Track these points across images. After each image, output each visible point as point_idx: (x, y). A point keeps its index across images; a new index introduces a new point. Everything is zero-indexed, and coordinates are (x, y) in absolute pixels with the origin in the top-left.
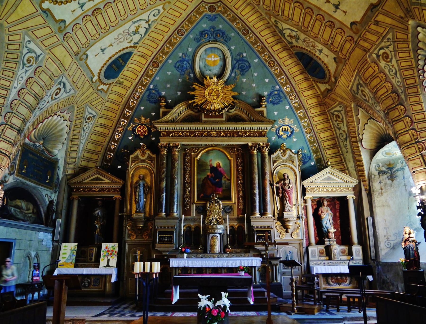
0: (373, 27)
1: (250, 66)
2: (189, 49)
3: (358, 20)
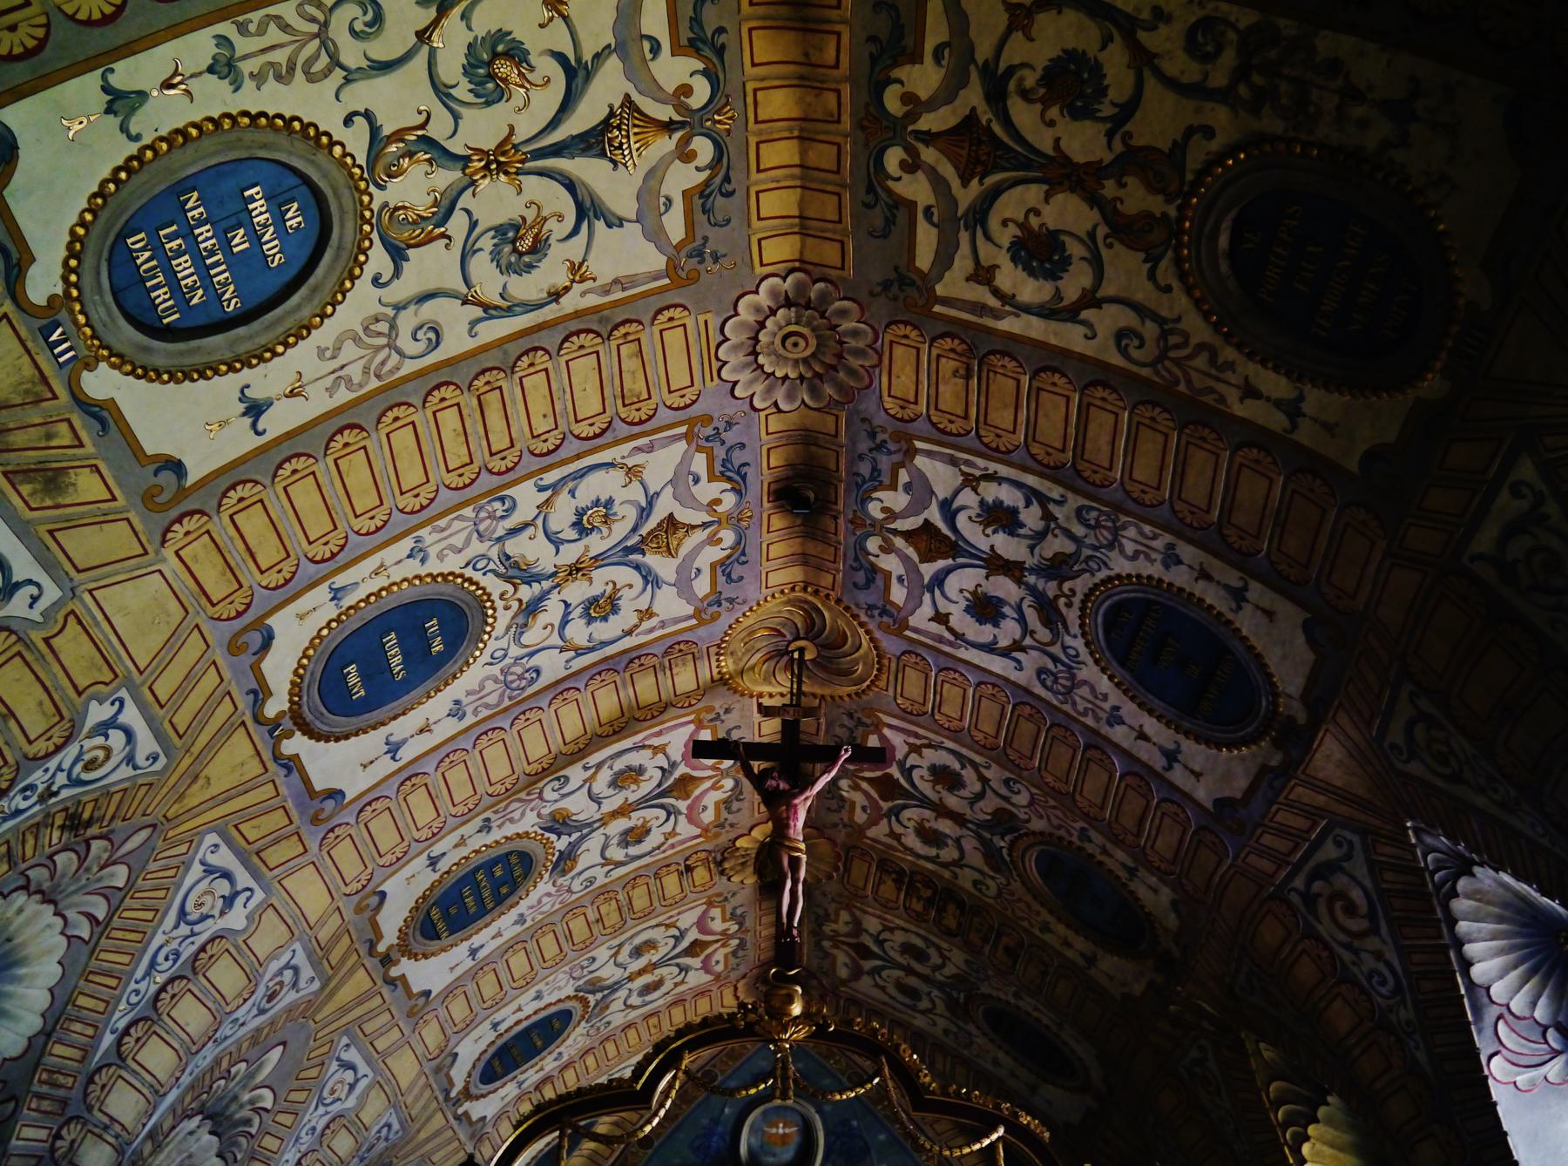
2: (727, 1110)
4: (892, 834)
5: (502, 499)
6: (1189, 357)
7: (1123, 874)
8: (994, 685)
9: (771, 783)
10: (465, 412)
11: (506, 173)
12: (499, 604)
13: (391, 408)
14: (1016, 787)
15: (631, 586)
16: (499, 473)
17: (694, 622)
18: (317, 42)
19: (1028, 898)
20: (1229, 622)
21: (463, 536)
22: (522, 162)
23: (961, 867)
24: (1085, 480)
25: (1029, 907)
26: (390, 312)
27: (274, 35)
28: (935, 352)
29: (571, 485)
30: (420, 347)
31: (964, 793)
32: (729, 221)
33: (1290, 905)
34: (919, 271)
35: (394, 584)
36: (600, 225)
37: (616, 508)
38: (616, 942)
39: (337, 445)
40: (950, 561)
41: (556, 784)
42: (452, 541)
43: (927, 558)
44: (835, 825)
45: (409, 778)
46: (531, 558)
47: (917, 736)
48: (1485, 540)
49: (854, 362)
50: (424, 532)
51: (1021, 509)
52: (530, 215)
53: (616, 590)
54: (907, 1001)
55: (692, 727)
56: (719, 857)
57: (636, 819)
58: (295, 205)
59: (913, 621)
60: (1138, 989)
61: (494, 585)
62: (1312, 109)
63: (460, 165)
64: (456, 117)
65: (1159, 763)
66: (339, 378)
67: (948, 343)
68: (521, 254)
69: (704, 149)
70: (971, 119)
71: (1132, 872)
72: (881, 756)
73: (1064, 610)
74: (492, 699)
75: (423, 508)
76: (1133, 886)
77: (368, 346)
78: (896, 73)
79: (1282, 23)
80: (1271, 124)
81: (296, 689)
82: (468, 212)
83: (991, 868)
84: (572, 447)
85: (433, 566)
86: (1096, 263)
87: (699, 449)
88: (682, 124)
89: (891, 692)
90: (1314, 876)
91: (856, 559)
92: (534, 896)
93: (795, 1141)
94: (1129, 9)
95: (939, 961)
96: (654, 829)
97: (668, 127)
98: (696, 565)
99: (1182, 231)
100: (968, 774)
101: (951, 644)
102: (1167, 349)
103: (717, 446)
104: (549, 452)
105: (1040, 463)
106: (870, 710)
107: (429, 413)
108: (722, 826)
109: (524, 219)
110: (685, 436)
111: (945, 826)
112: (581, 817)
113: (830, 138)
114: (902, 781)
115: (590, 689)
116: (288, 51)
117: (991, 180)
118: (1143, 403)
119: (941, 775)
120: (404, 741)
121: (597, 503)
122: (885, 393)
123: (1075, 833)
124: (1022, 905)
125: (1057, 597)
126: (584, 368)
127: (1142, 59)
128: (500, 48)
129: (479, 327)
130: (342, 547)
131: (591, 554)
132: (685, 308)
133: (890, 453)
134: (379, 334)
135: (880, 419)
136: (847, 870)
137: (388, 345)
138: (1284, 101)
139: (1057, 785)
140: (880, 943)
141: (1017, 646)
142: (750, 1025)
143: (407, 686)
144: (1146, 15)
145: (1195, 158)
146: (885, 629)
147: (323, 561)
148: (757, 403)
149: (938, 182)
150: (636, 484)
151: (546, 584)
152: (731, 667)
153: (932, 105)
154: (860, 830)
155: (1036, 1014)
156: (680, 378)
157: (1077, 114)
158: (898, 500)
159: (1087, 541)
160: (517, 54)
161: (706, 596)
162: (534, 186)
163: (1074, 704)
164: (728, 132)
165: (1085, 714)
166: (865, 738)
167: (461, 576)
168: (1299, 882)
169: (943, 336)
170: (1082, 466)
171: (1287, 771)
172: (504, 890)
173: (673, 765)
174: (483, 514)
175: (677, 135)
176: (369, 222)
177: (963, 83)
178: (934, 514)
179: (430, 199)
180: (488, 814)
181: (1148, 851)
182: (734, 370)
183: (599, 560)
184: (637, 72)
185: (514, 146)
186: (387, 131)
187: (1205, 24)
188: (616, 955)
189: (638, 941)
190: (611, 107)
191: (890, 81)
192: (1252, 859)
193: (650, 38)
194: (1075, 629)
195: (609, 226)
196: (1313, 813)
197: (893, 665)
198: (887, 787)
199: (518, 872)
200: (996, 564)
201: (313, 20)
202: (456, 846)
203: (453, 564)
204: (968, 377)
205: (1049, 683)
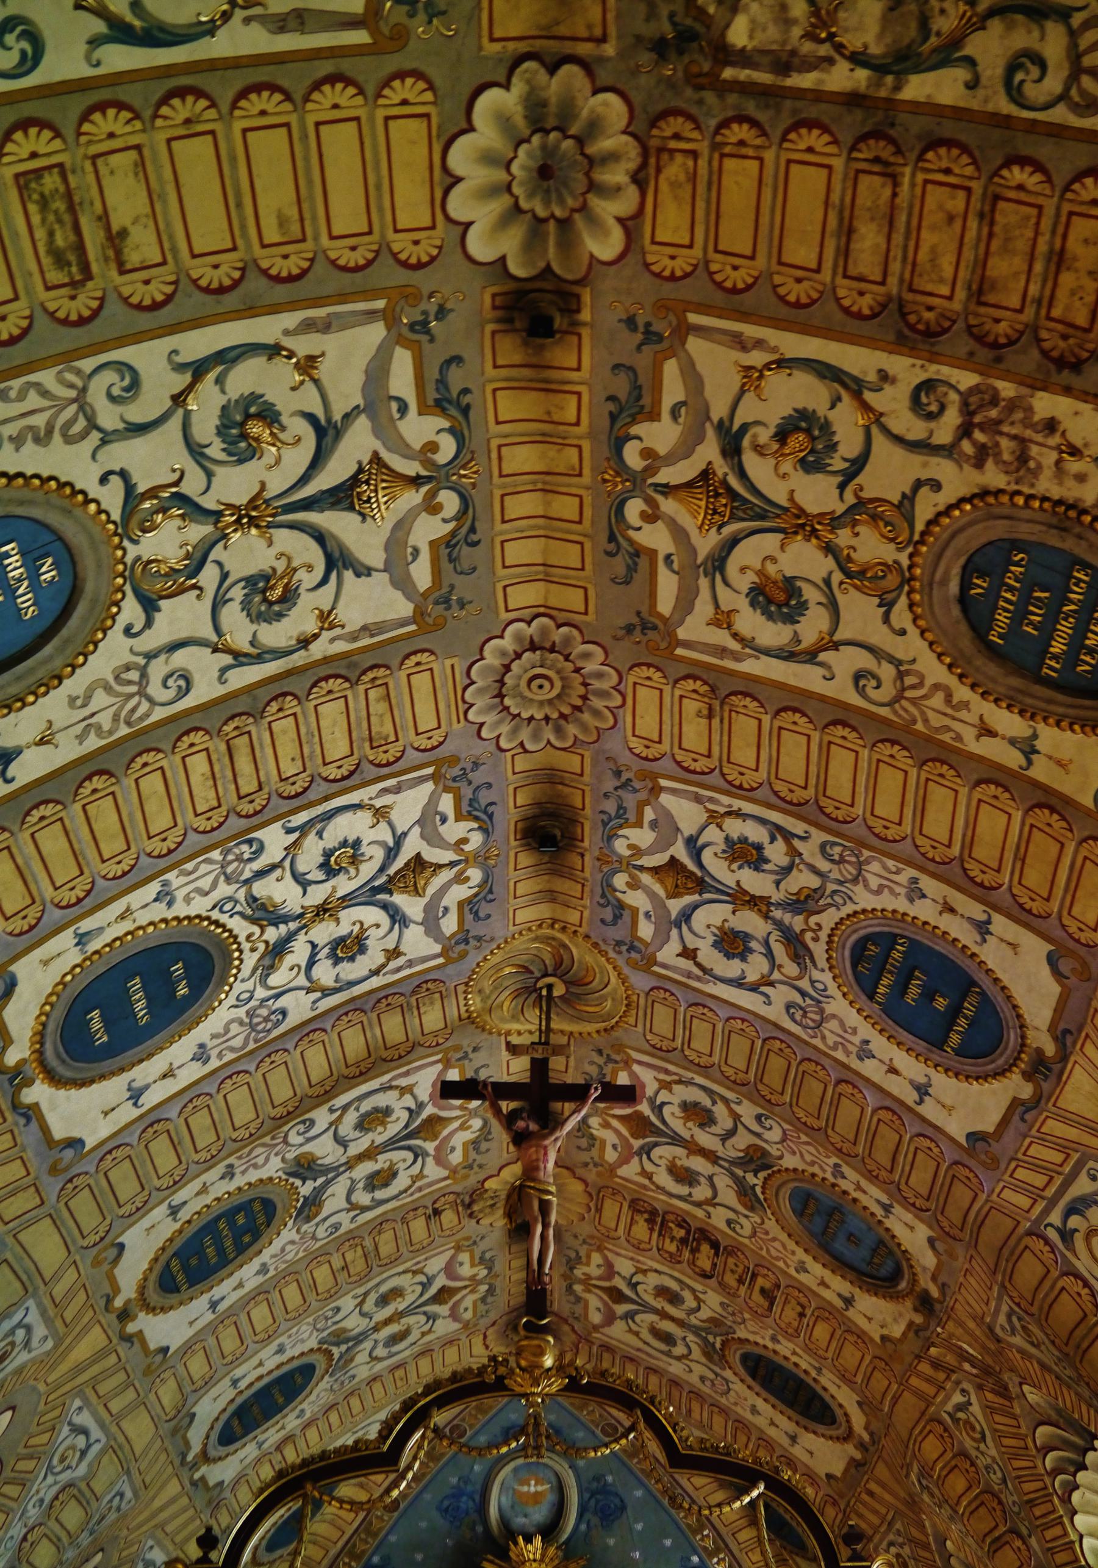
0: (864, 1496)
1: (623, 1508)
2: (476, 1468)
3: (839, 1474)
4: (644, 1173)
5: (250, 842)
6: (925, 697)
7: (879, 1212)
8: (743, 1020)
9: (521, 1124)
10: (214, 757)
11: (257, 527)
12: (246, 946)
13: (140, 754)
14: (768, 1123)
15: (378, 926)
16: (247, 816)
17: (441, 960)
18: (74, 407)
19: (783, 1237)
20: (974, 955)
21: (210, 879)
22: (273, 515)
23: (715, 1205)
24: (828, 816)
25: (784, 1246)
26: (142, 661)
27: (33, 400)
28: (677, 693)
29: (319, 826)
30: (171, 694)
31: (714, 1129)
32: (474, 569)
33: (1047, 1242)
34: (660, 616)
35: (140, 928)
36: (348, 574)
37: (364, 849)
38: (361, 1290)
39: (86, 791)
40: (696, 897)
41: (301, 1128)
42: (200, 884)
43: (674, 895)
44: (586, 1165)
45: (151, 1125)
46: (278, 899)
47: (667, 1072)
49: (597, 703)
50: (170, 876)
51: (766, 845)
52: (280, 567)
53: (363, 930)
54: (663, 1347)
55: (440, 1066)
56: (467, 1200)
57: (382, 1162)
58: (50, 560)
59: (661, 956)
60: (897, 1331)
61: (240, 927)
62: (1032, 464)
63: (212, 519)
64: (209, 475)
65: (910, 1096)
66: (89, 727)
67: (690, 684)
68: (271, 604)
69: (450, 501)
70: (706, 474)
71: (887, 1209)
72: (629, 1094)
73: (811, 945)
74: (237, 1042)
75: (170, 852)
76: (888, 1223)
77: (118, 695)
78: (634, 430)
79: (1000, 384)
80: (994, 477)
81: (40, 1036)
82: (220, 564)
83: (745, 1206)
84: (321, 788)
85: (181, 909)
86: (833, 607)
87: (447, 789)
88: (429, 479)
89: (640, 1028)
90: (1070, 1211)
91: (603, 895)
92: (277, 1244)
93: (551, 1498)
94: (855, 372)
95: (694, 1304)
96: (401, 1173)
97: (416, 481)
98: (444, 903)
99: (913, 578)
100: (720, 1111)
101: (698, 979)
102: (904, 689)
103: (463, 785)
104: (297, 795)
105: (783, 799)
106: (619, 1047)
107: (177, 759)
108: (471, 1167)
109: (274, 570)
110: (433, 777)
111: (698, 1164)
112: (327, 1161)
113: (574, 491)
114: (653, 1119)
115: (338, 1029)
116: (47, 415)
117: (728, 530)
118: (882, 741)
119: (690, 1109)
120: (147, 1087)
121: (344, 844)
122: (629, 733)
123: (829, 1170)
124: (776, 1244)
125: (803, 931)
126: (331, 711)
128: (253, 410)
129: (229, 674)
130: (89, 892)
131: (340, 893)
132: (432, 653)
133: (635, 791)
134: (130, 682)
135: (625, 758)
136: (599, 1210)
137: (139, 693)
138: (1006, 457)
139: (810, 1121)
140: (634, 1286)
141: (767, 981)
142: (500, 1379)
143: (151, 1030)
144: (872, 377)
145: (924, 511)
146: (635, 966)
147: (68, 906)
148: (504, 744)
149: (679, 533)
150: (383, 825)
151: (293, 926)
152: (479, 1005)
153: (671, 459)
154: (612, 1169)
155: (794, 1359)
156: (427, 721)
158: (643, 837)
159: (832, 876)
160: (269, 416)
161: (453, 935)
162: (285, 538)
163: (824, 1038)
164: (474, 485)
165: (835, 1048)
166: (615, 1073)
167: (208, 918)
168: (1055, 1218)
169: (686, 677)
170: (823, 802)
171: (1037, 1102)
172: (247, 1239)
173: (421, 1106)
174: (230, 857)
175: (424, 489)
176: (122, 575)
177: (700, 439)
178: (679, 851)
179: (183, 552)
180: (232, 1160)
181: (903, 1187)
182: (479, 712)
183: (348, 901)
184: (383, 429)
185: (266, 501)
186: (141, 488)
187: (928, 386)
188: (361, 1304)
189: (384, 1289)
190: (360, 463)
191: (629, 438)
192: (1007, 1194)
193: (398, 399)
194: (822, 963)
195: (358, 575)
196: (1065, 1147)
197: (642, 1001)
198: (639, 1125)
199: (261, 1219)
200: (742, 899)
201: (72, 386)
202: (198, 1194)
203: (200, 906)
204: (710, 717)
205: (798, 1017)
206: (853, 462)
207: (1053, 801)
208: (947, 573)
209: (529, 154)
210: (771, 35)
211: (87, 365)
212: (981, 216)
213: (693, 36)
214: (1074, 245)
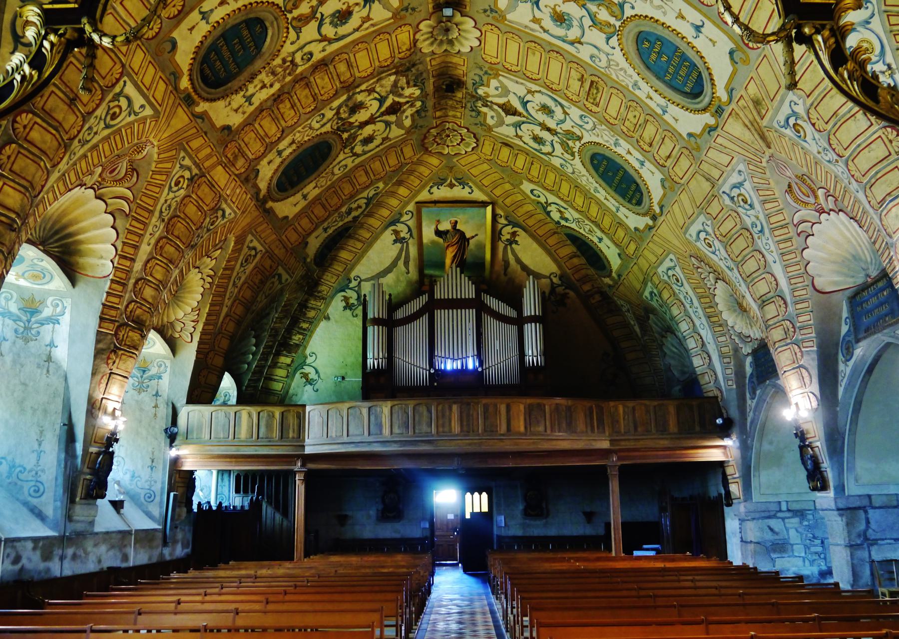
48: (130, 90)
64: (581, 19)
80: (278, 61)
127: (324, 39)
144: (327, 48)
145: (292, 34)
157: (338, 11)
186: (604, 36)
187: (309, 60)
206: (323, 25)
207: (182, 15)
208: (273, 27)
209: (452, 34)
210: (384, 82)
211: (602, 70)
212: (316, 94)
213: (406, 71)
214: (292, 111)
